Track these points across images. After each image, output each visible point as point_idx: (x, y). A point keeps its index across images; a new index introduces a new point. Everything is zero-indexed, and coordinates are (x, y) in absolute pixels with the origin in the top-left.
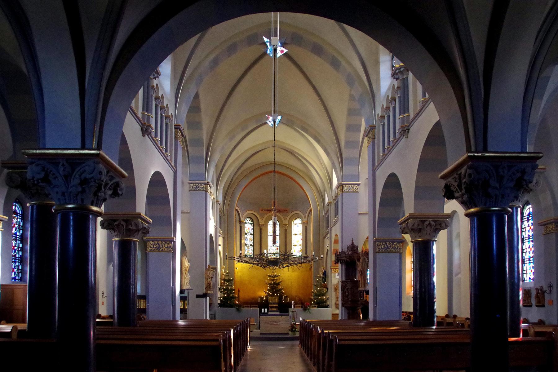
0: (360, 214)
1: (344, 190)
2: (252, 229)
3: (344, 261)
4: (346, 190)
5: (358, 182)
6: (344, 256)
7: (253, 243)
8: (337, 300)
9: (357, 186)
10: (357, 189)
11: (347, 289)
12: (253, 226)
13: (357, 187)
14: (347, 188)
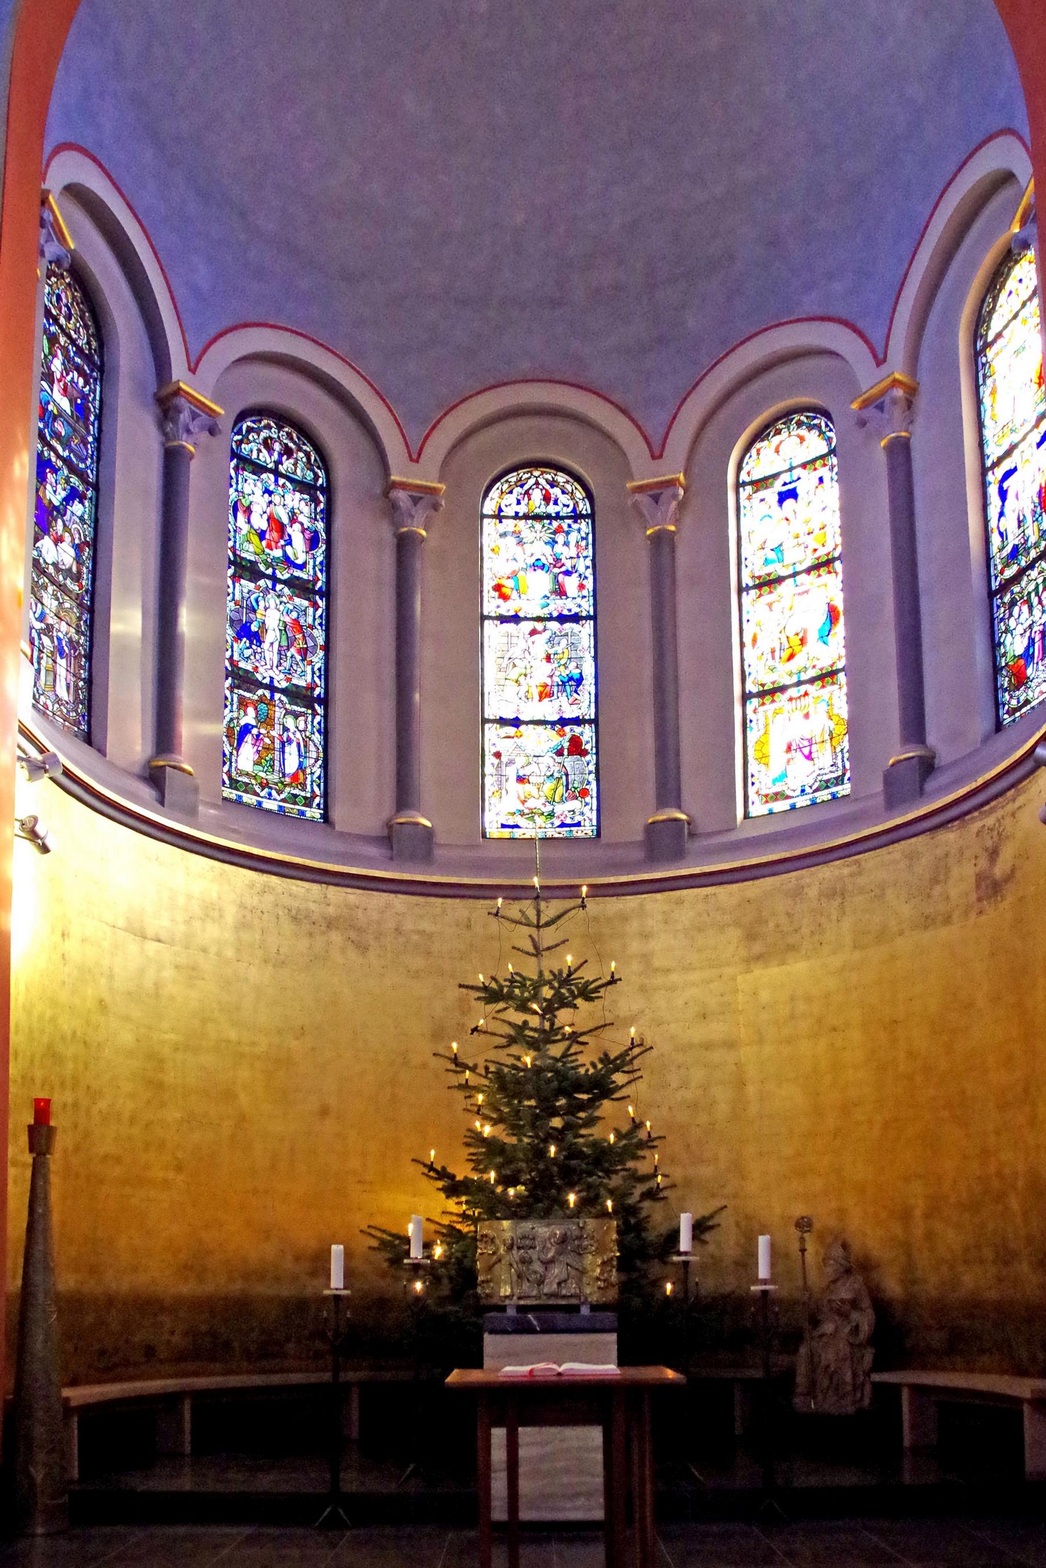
2: (313, 543)
7: (327, 673)
12: (328, 516)
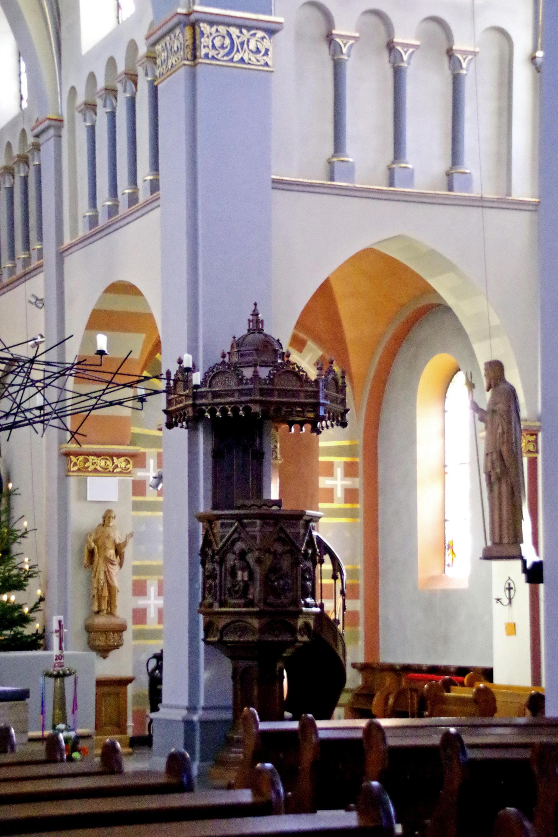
0: (279, 185)
1: (203, 51)
3: (213, 412)
4: (212, 53)
5: (270, 13)
6: (233, 385)
8: (96, 608)
9: (263, 38)
10: (267, 51)
11: (242, 555)
13: (267, 43)
14: (218, 42)
